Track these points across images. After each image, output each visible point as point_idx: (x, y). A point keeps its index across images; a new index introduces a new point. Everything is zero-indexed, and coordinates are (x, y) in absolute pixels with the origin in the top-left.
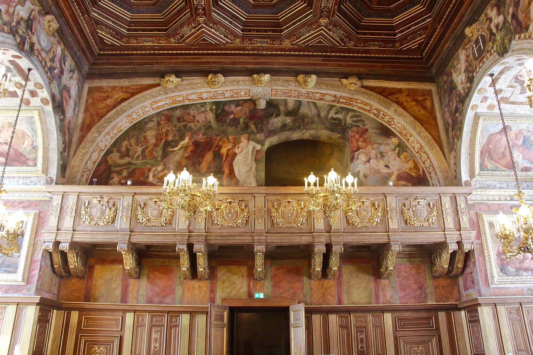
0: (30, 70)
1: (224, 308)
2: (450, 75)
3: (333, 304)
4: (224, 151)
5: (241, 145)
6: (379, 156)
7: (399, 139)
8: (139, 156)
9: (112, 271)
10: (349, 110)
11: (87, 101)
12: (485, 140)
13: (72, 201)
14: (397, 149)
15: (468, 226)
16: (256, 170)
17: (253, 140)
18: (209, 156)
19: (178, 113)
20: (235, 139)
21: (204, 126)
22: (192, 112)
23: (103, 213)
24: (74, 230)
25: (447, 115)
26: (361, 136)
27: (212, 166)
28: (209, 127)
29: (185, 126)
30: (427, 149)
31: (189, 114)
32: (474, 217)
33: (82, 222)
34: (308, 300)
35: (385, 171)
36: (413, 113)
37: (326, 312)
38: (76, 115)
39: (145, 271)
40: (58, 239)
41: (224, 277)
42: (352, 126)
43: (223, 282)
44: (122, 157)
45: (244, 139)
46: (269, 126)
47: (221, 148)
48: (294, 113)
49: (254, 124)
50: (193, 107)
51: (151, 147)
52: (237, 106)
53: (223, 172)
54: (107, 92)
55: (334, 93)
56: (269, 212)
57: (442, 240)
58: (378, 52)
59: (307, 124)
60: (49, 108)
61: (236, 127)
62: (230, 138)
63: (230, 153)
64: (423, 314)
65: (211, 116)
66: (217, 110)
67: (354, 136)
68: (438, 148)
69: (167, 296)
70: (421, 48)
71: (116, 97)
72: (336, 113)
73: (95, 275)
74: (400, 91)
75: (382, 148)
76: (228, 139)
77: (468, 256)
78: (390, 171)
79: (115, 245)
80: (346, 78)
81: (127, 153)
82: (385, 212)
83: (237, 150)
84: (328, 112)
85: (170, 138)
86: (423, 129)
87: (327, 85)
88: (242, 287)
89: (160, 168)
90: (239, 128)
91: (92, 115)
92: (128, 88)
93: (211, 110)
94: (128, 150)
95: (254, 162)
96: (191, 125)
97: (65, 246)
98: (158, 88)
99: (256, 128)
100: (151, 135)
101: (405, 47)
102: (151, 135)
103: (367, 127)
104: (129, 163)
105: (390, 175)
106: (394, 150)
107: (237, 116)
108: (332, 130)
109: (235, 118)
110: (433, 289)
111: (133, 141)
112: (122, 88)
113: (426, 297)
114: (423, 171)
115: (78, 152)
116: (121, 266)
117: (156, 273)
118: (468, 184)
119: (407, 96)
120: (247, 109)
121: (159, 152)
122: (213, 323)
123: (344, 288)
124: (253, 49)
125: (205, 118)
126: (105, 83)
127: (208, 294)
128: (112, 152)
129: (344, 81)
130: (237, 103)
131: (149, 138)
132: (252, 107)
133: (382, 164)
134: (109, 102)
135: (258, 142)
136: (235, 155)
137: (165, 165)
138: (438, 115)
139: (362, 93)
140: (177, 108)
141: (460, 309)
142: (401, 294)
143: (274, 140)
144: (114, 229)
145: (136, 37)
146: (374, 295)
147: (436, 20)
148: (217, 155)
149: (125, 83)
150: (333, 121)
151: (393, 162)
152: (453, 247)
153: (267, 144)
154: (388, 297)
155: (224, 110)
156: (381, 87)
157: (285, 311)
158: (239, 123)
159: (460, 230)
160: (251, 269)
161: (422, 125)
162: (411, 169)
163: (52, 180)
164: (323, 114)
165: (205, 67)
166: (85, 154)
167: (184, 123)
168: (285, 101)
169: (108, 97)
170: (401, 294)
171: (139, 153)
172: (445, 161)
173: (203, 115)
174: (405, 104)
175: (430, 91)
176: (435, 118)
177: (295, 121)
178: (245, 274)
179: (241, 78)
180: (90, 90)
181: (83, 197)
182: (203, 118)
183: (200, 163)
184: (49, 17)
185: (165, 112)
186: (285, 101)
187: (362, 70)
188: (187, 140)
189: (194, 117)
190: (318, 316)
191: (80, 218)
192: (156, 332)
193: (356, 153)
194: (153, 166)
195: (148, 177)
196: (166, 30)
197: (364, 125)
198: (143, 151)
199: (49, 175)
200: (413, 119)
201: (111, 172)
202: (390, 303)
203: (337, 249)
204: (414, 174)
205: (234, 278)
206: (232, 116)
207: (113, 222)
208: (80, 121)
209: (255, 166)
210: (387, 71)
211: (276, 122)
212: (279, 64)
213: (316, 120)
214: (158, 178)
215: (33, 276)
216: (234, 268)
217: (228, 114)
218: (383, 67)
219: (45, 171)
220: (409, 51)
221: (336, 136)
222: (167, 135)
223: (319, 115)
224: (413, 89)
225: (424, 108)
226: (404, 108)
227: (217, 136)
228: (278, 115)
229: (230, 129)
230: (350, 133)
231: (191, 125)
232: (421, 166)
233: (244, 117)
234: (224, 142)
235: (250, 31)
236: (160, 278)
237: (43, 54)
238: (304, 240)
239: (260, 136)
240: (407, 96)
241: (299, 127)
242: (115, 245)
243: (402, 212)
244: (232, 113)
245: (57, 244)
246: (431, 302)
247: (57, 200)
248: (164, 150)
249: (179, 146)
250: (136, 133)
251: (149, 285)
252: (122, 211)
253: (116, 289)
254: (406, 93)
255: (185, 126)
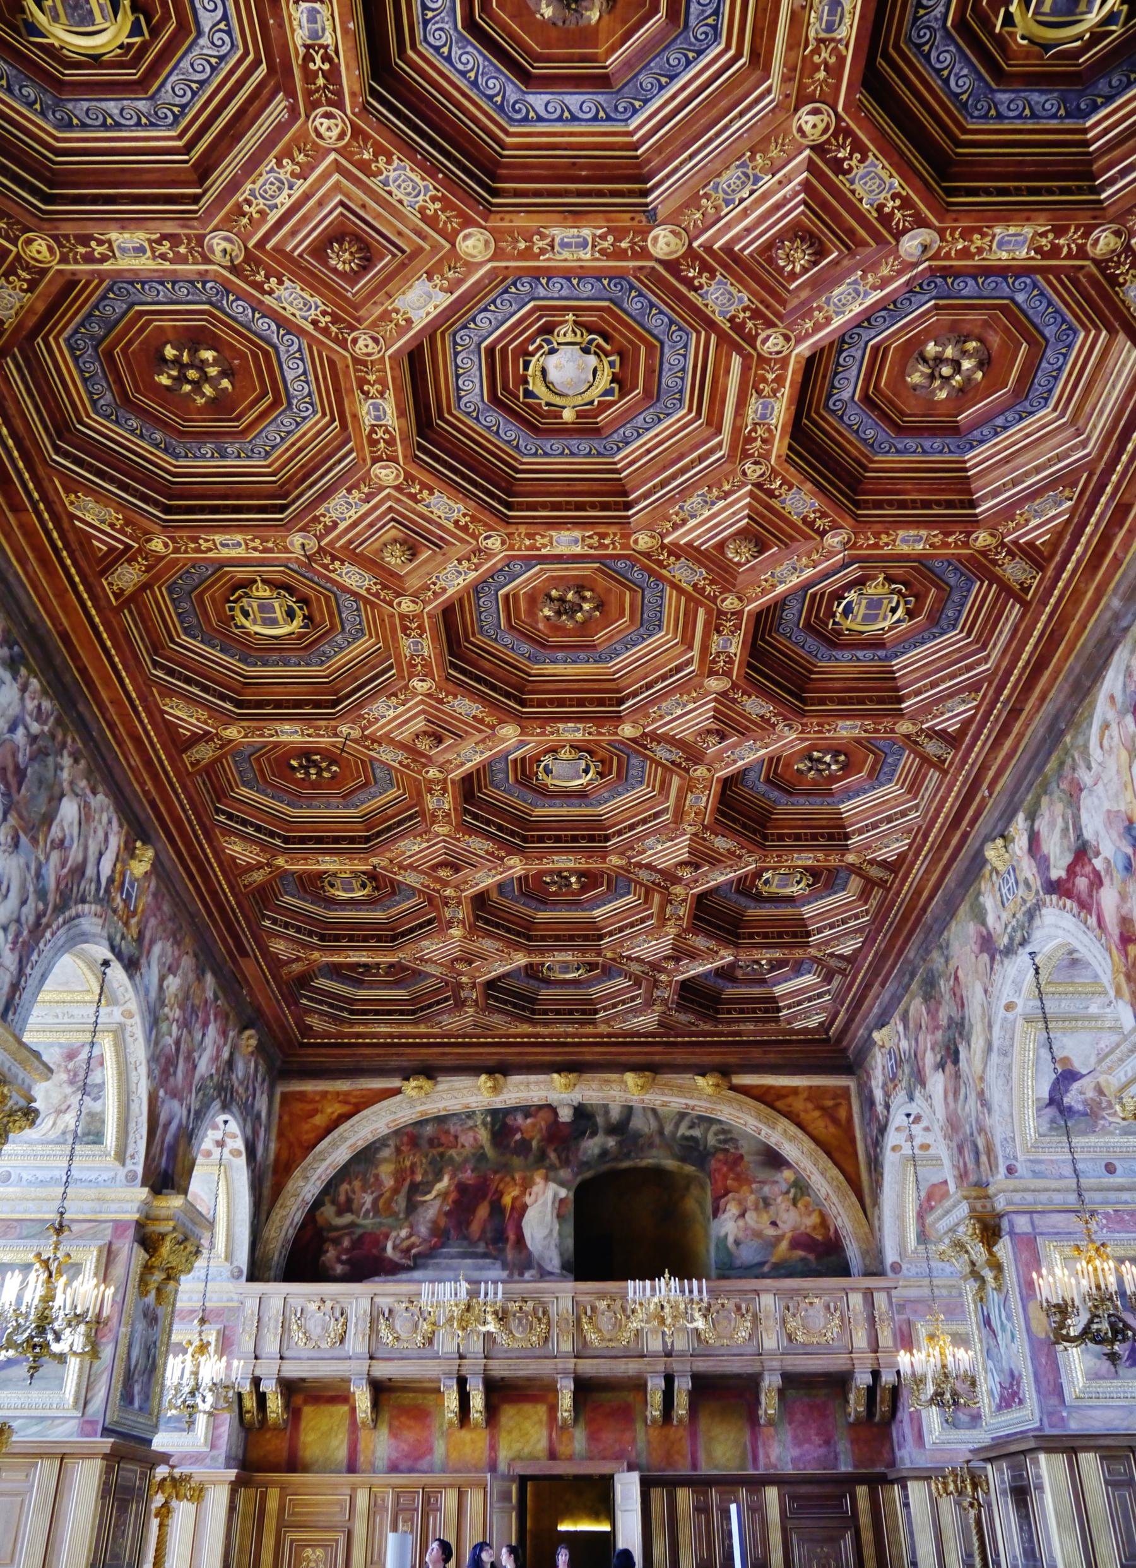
0: (226, 1122)
1: (511, 1478)
2: (869, 1077)
3: (686, 1472)
4: (507, 1200)
5: (535, 1189)
6: (761, 1204)
7: (796, 1172)
8: (367, 1211)
9: (331, 1416)
10: (711, 1121)
11: (281, 1118)
12: (923, 1194)
13: (275, 1305)
14: (793, 1191)
15: (891, 1344)
16: (560, 1234)
17: (555, 1181)
18: (483, 1211)
19: (429, 1130)
20: (524, 1179)
21: (474, 1155)
22: (452, 1130)
23: (325, 1329)
24: (282, 1358)
25: (869, 1140)
26: (731, 1169)
27: (489, 1228)
28: (481, 1157)
29: (442, 1155)
30: (834, 1199)
31: (447, 1132)
32: (905, 1327)
33: (292, 1344)
34: (643, 1460)
35: (771, 1232)
36: (815, 1132)
37: (672, 1484)
38: (266, 1148)
39: (385, 1416)
40: (257, 1373)
41: (512, 1424)
42: (717, 1150)
43: (510, 1432)
44: (340, 1213)
45: (538, 1179)
46: (580, 1153)
47: (501, 1194)
48: (620, 1129)
49: (555, 1150)
50: (455, 1120)
51: (388, 1194)
52: (526, 1117)
53: (506, 1240)
54: (312, 1101)
55: (683, 1101)
56: (578, 1320)
57: (848, 1367)
58: (754, 1033)
59: (642, 1149)
60: (242, 1161)
61: (526, 1157)
62: (517, 1176)
63: (517, 1204)
64: (828, 1490)
65: (483, 1135)
66: (493, 1123)
67: (719, 1170)
68: (854, 1199)
69: (420, 1457)
70: (824, 1027)
71: (330, 1110)
72: (691, 1127)
73: (303, 1424)
74: (795, 1091)
75: (766, 1189)
76: (513, 1179)
77: (895, 1391)
78: (779, 1232)
79: (349, 1381)
80: (703, 1075)
81: (347, 1207)
82: (756, 1320)
83: (528, 1200)
84: (677, 1125)
85: (419, 1178)
86: (830, 1164)
87: (671, 1087)
88: (539, 1441)
89: (404, 1233)
90: (531, 1158)
91: (291, 1146)
92: (347, 1094)
93: (484, 1124)
94: (349, 1201)
95: (555, 1221)
96: (453, 1152)
97: (269, 1386)
98: (399, 1098)
99: (559, 1157)
100: (386, 1173)
101: (797, 1025)
102: (386, 1173)
103: (742, 1151)
104: (353, 1225)
105: (779, 1239)
106: (788, 1192)
107: (527, 1136)
108: (683, 1160)
109: (523, 1140)
110: (848, 1446)
111: (357, 1184)
112: (338, 1094)
113: (836, 1458)
114: (836, 1231)
115: (273, 1214)
116: (345, 1408)
117: (403, 1419)
118: (896, 1268)
119: (808, 1099)
120: (543, 1123)
121: (401, 1203)
122: (496, 1505)
123: (701, 1442)
124: (551, 1036)
125: (475, 1139)
126: (310, 1087)
127: (487, 1453)
128: (323, 1204)
129: (700, 1081)
130: (527, 1111)
131: (383, 1177)
132: (551, 1118)
133: (765, 1219)
134: (319, 1120)
135: (562, 1184)
136: (525, 1207)
137: (411, 1227)
138: (858, 1135)
139: (730, 1101)
140: (427, 1121)
141: (892, 1482)
142: (795, 1452)
143: (588, 1174)
144: (343, 1354)
145: (365, 1023)
146: (750, 1457)
147: (839, 999)
148: (497, 1208)
149: (343, 1085)
150: (685, 1143)
151: (785, 1216)
152: (863, 1379)
153: (579, 1179)
154: (773, 1459)
155: (504, 1125)
156: (762, 1086)
157: (612, 1477)
158: (530, 1148)
159: (876, 1352)
160: (553, 1409)
161: (829, 1154)
162: (814, 1228)
163: (241, 1271)
164: (668, 1129)
165: (475, 1061)
166: (284, 1218)
167: (441, 1150)
168: (606, 1106)
169: (315, 1112)
170: (795, 1452)
171: (368, 1205)
172: (864, 1221)
173: (471, 1134)
174: (802, 1115)
175: (848, 1088)
176: (853, 1140)
177: (620, 1144)
178: (545, 1418)
179: (533, 1078)
180: (284, 1096)
181: (290, 1300)
182: (471, 1140)
183: (468, 1223)
184: (248, 1033)
185: (409, 1129)
186: (606, 1106)
187: (732, 1059)
188: (446, 1181)
189: (456, 1137)
190: (659, 1490)
191: (290, 1337)
192: (404, 1521)
193: (723, 1201)
194: (392, 1228)
195: (384, 1249)
196: (413, 1012)
197: (737, 1148)
198: (375, 1202)
199: (236, 1264)
200: (813, 1146)
201: (324, 1241)
202: (775, 1467)
203: (683, 1385)
204: (819, 1238)
205: (527, 1425)
206: (518, 1136)
207: (342, 1341)
208: (272, 1156)
209: (557, 1227)
210: (772, 1058)
211: (592, 1146)
212: (593, 1054)
213: (657, 1140)
214: (402, 1251)
215: (220, 1437)
216: (528, 1408)
217: (513, 1130)
218: (765, 1052)
219: (229, 1256)
220: (805, 1031)
221: (689, 1169)
222: (413, 1172)
223: (661, 1132)
224: (818, 1087)
225: (835, 1121)
226: (800, 1125)
227: (496, 1172)
228: (594, 1134)
229: (517, 1161)
230: (713, 1164)
231: (453, 1152)
232: (831, 1222)
233: (538, 1137)
234: (507, 1184)
235: (545, 1012)
236: (410, 1428)
237: (241, 1090)
238: (630, 1368)
239: (565, 1174)
240: (808, 1099)
241: (627, 1156)
242: (346, 1381)
243: (784, 1322)
244: (519, 1129)
245: (256, 1381)
246: (845, 1468)
247: (252, 1304)
248: (409, 1199)
249: (434, 1193)
250: (361, 1168)
251: (392, 1441)
252: (356, 1324)
253: (338, 1448)
254: (805, 1095)
255: (442, 1155)
